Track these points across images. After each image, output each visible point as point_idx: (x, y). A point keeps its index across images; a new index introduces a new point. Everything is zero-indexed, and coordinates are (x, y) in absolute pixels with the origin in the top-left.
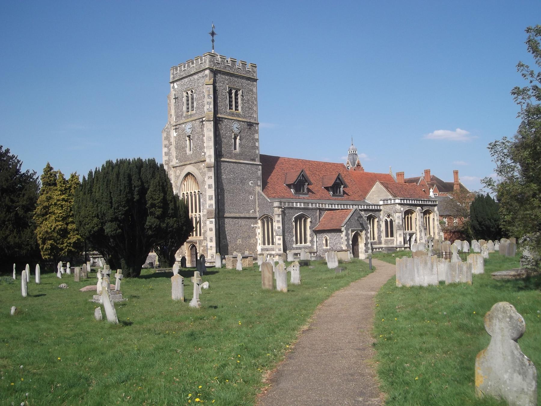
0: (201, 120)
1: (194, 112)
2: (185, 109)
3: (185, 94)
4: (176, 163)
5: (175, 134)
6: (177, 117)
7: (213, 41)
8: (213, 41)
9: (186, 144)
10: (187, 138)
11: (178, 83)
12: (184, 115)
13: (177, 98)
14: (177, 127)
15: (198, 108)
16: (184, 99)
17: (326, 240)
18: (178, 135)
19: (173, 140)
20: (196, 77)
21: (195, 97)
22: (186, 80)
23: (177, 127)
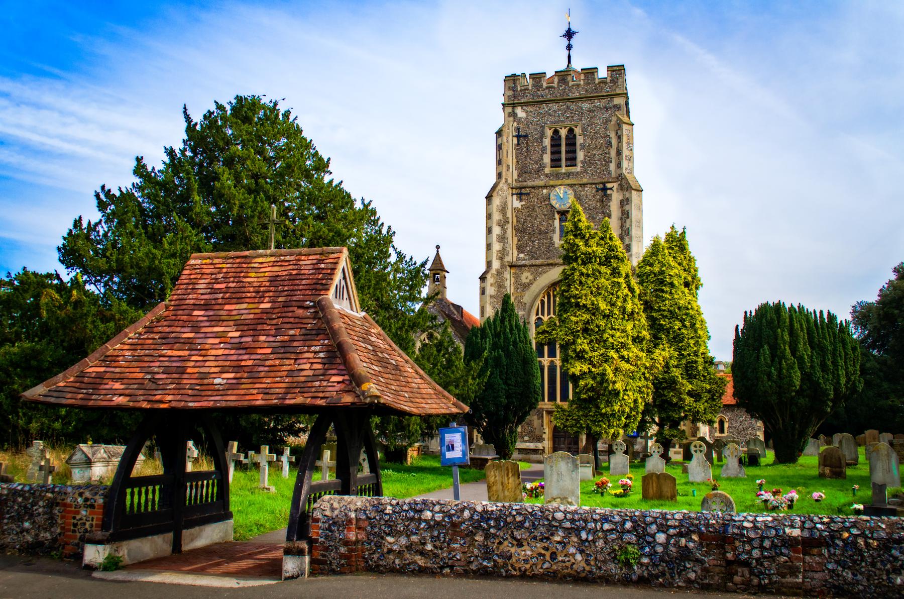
0: (601, 186)
1: (578, 169)
2: (547, 158)
3: (549, 133)
4: (518, 259)
5: (517, 204)
6: (523, 171)
7: (569, 47)
8: (569, 47)
9: (552, 225)
10: (557, 216)
11: (529, 109)
12: (547, 170)
13: (526, 136)
14: (523, 191)
15: (587, 163)
16: (547, 142)
17: (721, 423)
18: (530, 208)
19: (509, 215)
20: (586, 106)
21: (580, 140)
22: (555, 107)
23: (523, 191)
